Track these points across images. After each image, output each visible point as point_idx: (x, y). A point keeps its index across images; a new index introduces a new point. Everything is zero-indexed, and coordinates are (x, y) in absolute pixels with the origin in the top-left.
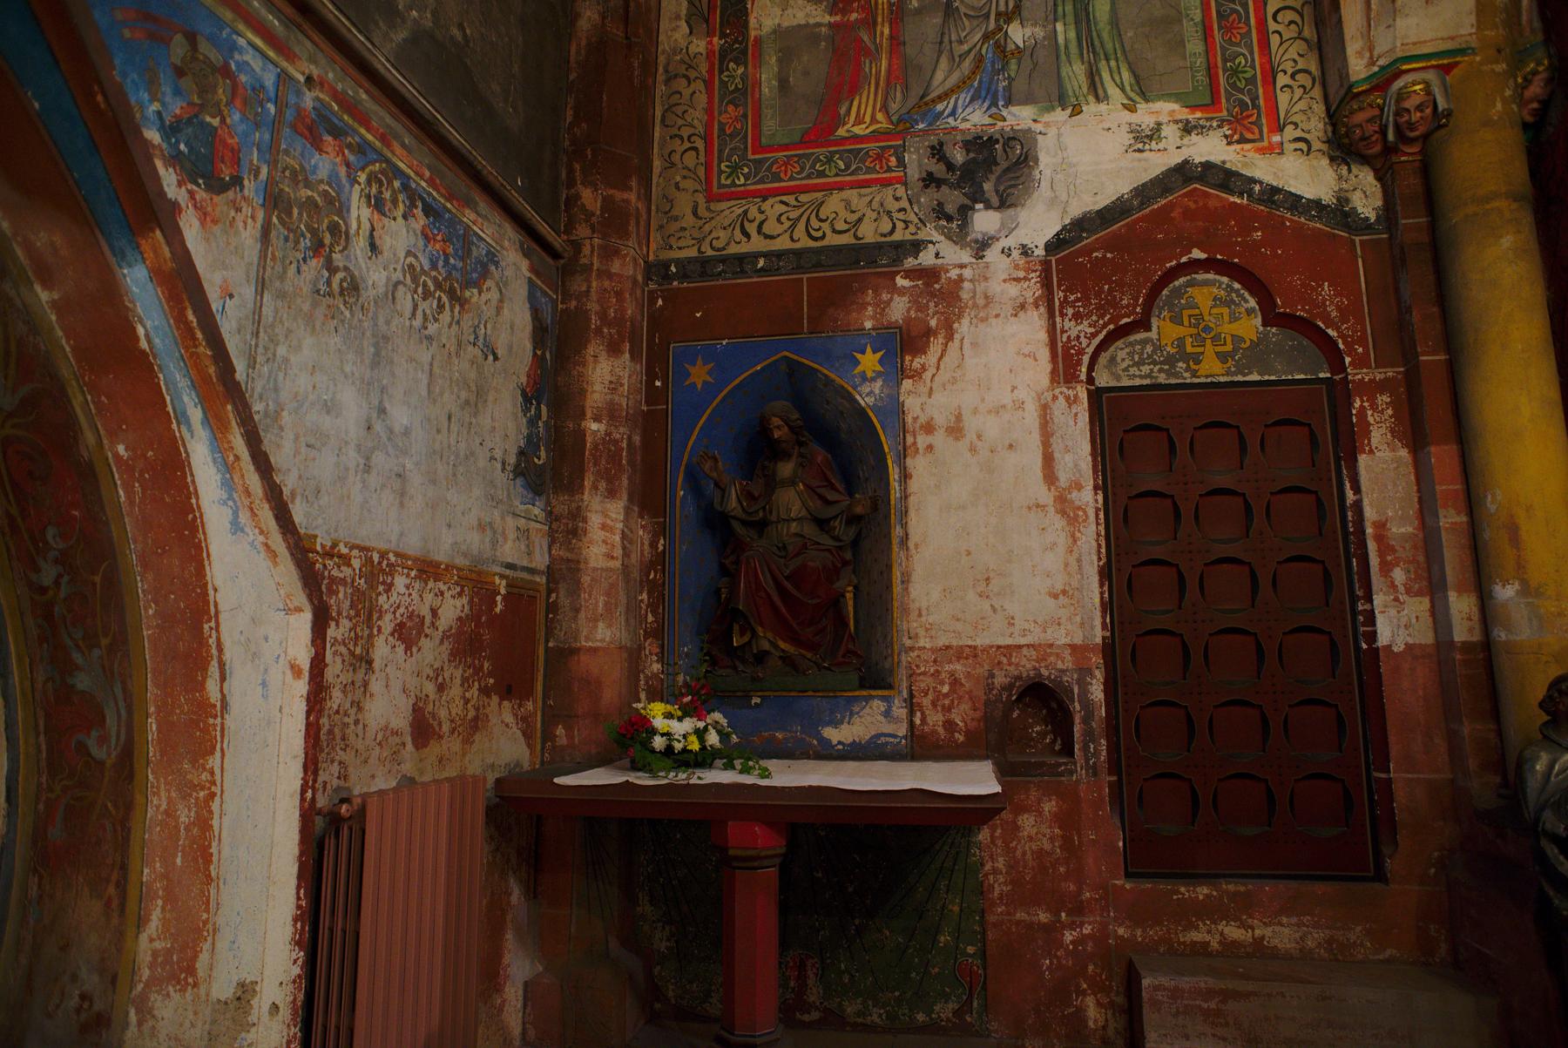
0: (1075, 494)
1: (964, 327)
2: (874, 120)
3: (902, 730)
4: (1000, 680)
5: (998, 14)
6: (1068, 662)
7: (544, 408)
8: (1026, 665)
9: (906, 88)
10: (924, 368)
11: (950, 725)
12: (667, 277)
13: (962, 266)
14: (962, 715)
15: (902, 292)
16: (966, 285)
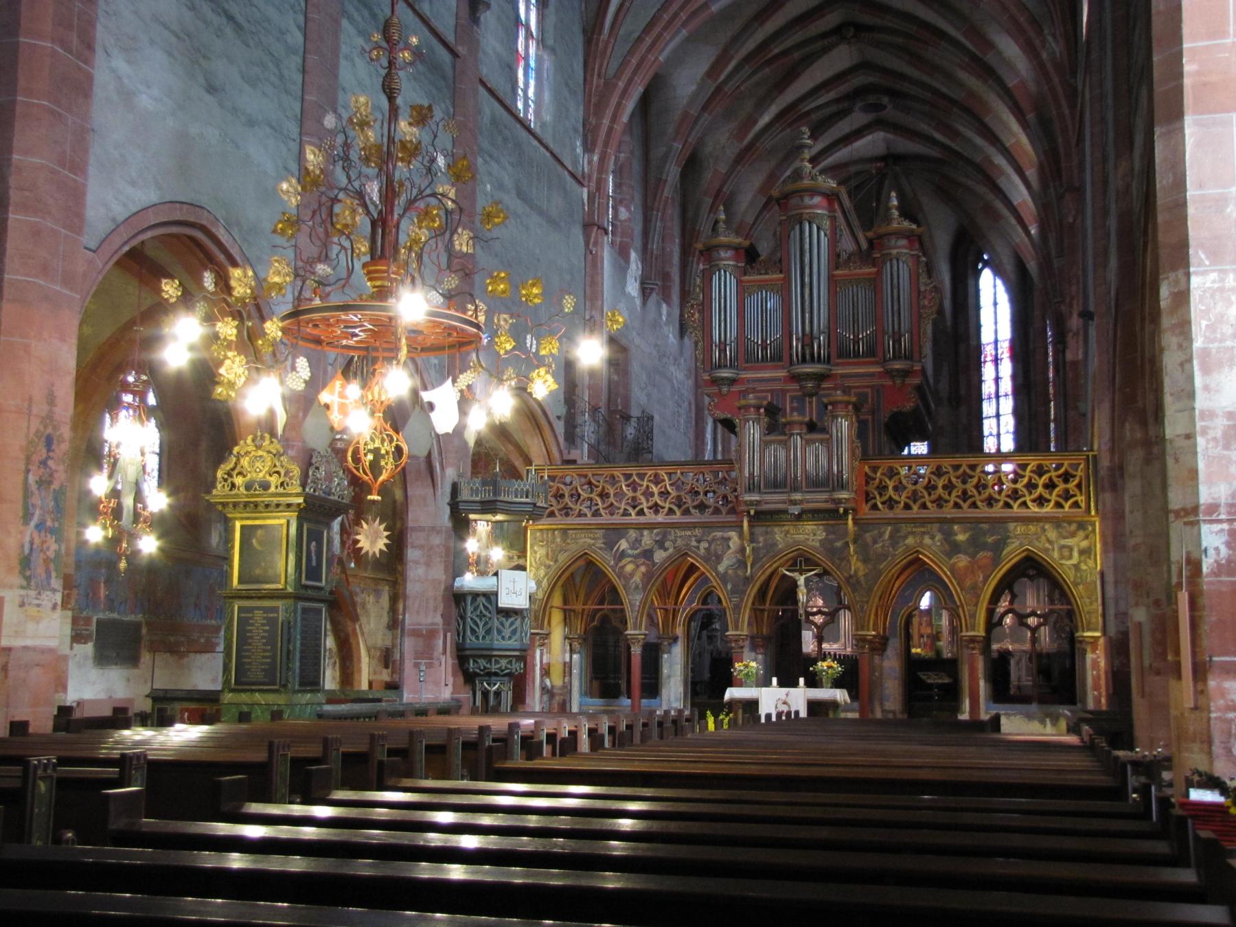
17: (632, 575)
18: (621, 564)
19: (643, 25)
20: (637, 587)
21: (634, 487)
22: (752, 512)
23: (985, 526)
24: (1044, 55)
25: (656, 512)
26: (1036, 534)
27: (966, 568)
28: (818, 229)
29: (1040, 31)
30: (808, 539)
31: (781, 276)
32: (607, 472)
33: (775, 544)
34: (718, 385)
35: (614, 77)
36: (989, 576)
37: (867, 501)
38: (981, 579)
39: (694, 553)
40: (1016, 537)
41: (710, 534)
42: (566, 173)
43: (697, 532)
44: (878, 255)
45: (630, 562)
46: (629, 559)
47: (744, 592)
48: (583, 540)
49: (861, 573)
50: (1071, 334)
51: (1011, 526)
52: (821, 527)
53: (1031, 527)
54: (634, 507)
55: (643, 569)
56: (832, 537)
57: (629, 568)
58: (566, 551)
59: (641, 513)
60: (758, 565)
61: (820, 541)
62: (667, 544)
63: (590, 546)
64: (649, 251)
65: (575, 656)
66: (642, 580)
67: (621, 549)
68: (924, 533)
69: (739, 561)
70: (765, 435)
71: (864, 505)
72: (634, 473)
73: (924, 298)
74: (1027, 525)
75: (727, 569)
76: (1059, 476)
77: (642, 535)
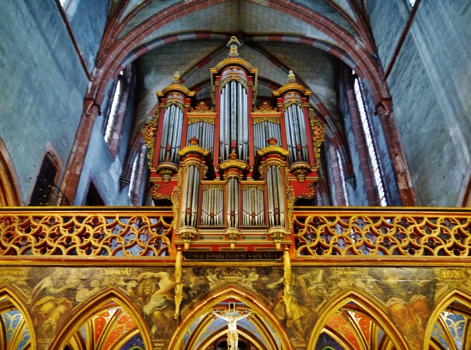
18: (38, 303)
19: (140, 23)
20: (51, 328)
21: (71, 228)
22: (187, 246)
23: (414, 270)
24: (357, 48)
26: (461, 278)
27: (403, 312)
28: (242, 85)
29: (353, 38)
30: (239, 281)
31: (216, 113)
32: (47, 215)
33: (206, 286)
34: (161, 176)
35: (121, 39)
36: (427, 319)
37: (297, 248)
38: (420, 323)
40: (443, 281)
41: (139, 273)
42: (78, 56)
43: (127, 271)
44: (282, 106)
47: (170, 339)
49: (296, 316)
50: (400, 174)
51: (437, 270)
52: (254, 269)
53: (454, 271)
54: (66, 247)
55: (62, 309)
56: (265, 279)
57: (47, 308)
59: (73, 252)
60: (186, 307)
61: (252, 282)
63: (11, 283)
64: (127, 165)
66: (58, 322)
67: (43, 288)
68: (356, 276)
69: (167, 301)
70: (205, 179)
71: (294, 250)
72: (74, 215)
73: (314, 130)
74: (451, 270)
75: (154, 309)
76: (465, 229)
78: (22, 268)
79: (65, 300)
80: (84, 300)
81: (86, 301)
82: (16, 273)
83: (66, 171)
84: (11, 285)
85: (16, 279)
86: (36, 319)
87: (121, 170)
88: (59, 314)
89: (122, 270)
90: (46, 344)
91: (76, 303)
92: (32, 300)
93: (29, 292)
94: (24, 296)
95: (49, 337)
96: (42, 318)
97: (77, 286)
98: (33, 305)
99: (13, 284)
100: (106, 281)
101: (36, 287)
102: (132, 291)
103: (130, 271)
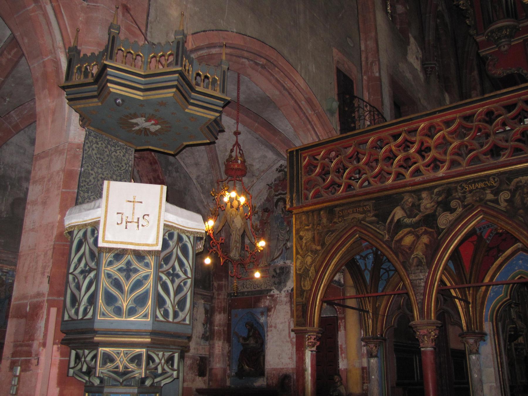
0: (293, 339)
1: (277, 307)
2: (265, 264)
3: (265, 384)
4: (281, 374)
5: (286, 240)
6: (291, 371)
7: (208, 325)
8: (284, 372)
9: (270, 257)
10: (271, 315)
11: (273, 382)
12: (231, 296)
13: (278, 294)
14: (275, 381)
15: (268, 299)
16: (278, 298)
17: (412, 247)
18: (397, 238)
20: (420, 263)
25: (436, 168)
39: (493, 209)
41: (510, 180)
45: (408, 233)
46: (408, 230)
48: (351, 217)
55: (425, 239)
57: (408, 240)
58: (333, 232)
62: (453, 204)
65: (373, 361)
67: (396, 219)
77: (420, 199)
78: (366, 203)
79: (425, 229)
80: (448, 225)
81: (452, 225)
82: (361, 209)
83: (362, 77)
84: (360, 223)
85: (363, 215)
86: (400, 255)
87: (420, 51)
88: (424, 245)
89: (485, 181)
90: (421, 279)
91: (440, 231)
92: (389, 235)
93: (383, 227)
94: (378, 233)
95: (421, 272)
96: (407, 252)
97: (435, 211)
98: (392, 241)
99: (363, 222)
100: (468, 198)
101: (388, 221)
102: (506, 204)
103: (496, 180)
